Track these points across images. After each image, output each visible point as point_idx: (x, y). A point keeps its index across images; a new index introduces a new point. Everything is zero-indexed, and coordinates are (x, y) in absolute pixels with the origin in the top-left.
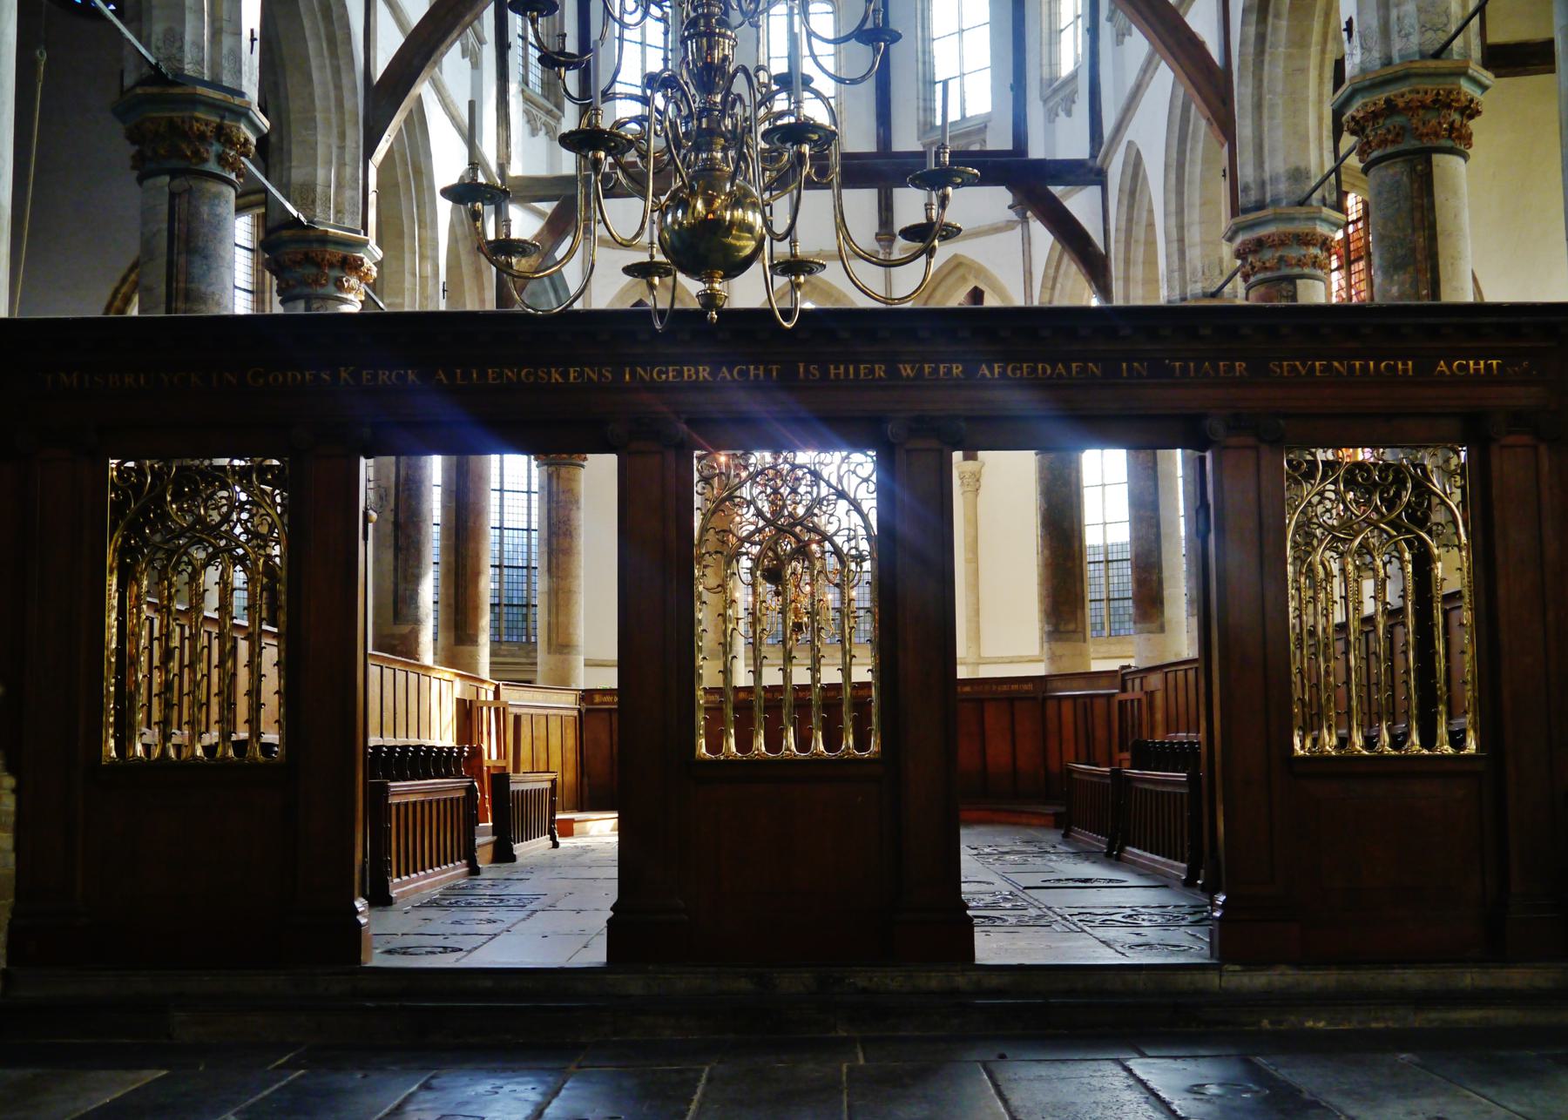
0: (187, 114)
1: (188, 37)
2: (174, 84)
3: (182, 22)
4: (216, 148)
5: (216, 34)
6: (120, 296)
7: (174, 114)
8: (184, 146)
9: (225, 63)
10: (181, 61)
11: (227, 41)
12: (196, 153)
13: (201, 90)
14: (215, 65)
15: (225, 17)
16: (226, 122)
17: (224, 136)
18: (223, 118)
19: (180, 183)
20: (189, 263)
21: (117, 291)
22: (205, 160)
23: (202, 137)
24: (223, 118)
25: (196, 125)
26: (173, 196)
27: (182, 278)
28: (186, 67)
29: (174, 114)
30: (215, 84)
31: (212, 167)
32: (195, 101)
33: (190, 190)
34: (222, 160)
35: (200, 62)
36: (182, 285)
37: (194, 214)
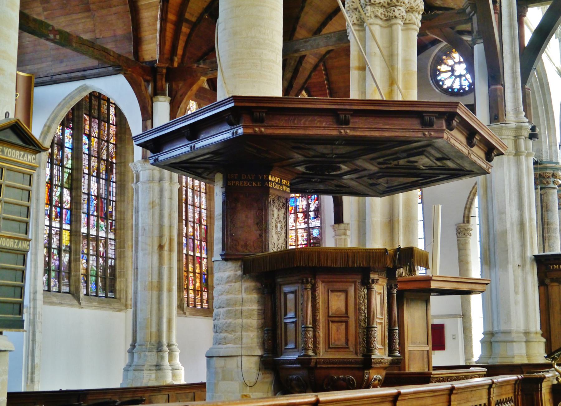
0: (544, 172)
1: (543, 150)
2: (540, 164)
3: (542, 146)
4: (552, 179)
5: (550, 147)
6: (472, 194)
7: (541, 172)
8: (544, 181)
9: (553, 155)
10: (542, 157)
11: (553, 148)
12: (547, 182)
13: (549, 165)
14: (551, 156)
15: (552, 141)
16: (555, 172)
17: (554, 175)
18: (554, 171)
19: (543, 191)
20: (547, 214)
21: (471, 192)
22: (549, 184)
23: (549, 177)
24: (554, 171)
25: (547, 174)
26: (541, 195)
27: (546, 218)
28: (544, 158)
29: (541, 172)
30: (551, 162)
31: (551, 185)
32: (546, 168)
33: (546, 193)
34: (554, 182)
35: (547, 157)
36: (546, 220)
37: (547, 200)
